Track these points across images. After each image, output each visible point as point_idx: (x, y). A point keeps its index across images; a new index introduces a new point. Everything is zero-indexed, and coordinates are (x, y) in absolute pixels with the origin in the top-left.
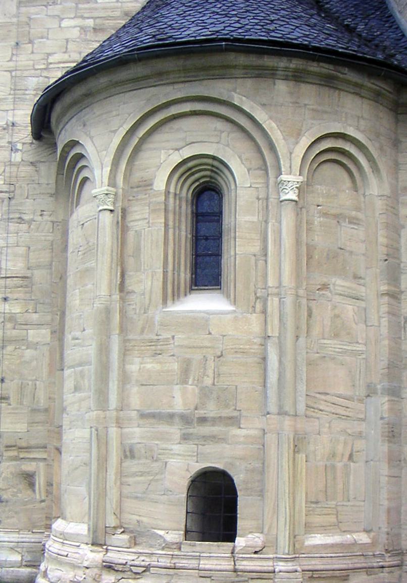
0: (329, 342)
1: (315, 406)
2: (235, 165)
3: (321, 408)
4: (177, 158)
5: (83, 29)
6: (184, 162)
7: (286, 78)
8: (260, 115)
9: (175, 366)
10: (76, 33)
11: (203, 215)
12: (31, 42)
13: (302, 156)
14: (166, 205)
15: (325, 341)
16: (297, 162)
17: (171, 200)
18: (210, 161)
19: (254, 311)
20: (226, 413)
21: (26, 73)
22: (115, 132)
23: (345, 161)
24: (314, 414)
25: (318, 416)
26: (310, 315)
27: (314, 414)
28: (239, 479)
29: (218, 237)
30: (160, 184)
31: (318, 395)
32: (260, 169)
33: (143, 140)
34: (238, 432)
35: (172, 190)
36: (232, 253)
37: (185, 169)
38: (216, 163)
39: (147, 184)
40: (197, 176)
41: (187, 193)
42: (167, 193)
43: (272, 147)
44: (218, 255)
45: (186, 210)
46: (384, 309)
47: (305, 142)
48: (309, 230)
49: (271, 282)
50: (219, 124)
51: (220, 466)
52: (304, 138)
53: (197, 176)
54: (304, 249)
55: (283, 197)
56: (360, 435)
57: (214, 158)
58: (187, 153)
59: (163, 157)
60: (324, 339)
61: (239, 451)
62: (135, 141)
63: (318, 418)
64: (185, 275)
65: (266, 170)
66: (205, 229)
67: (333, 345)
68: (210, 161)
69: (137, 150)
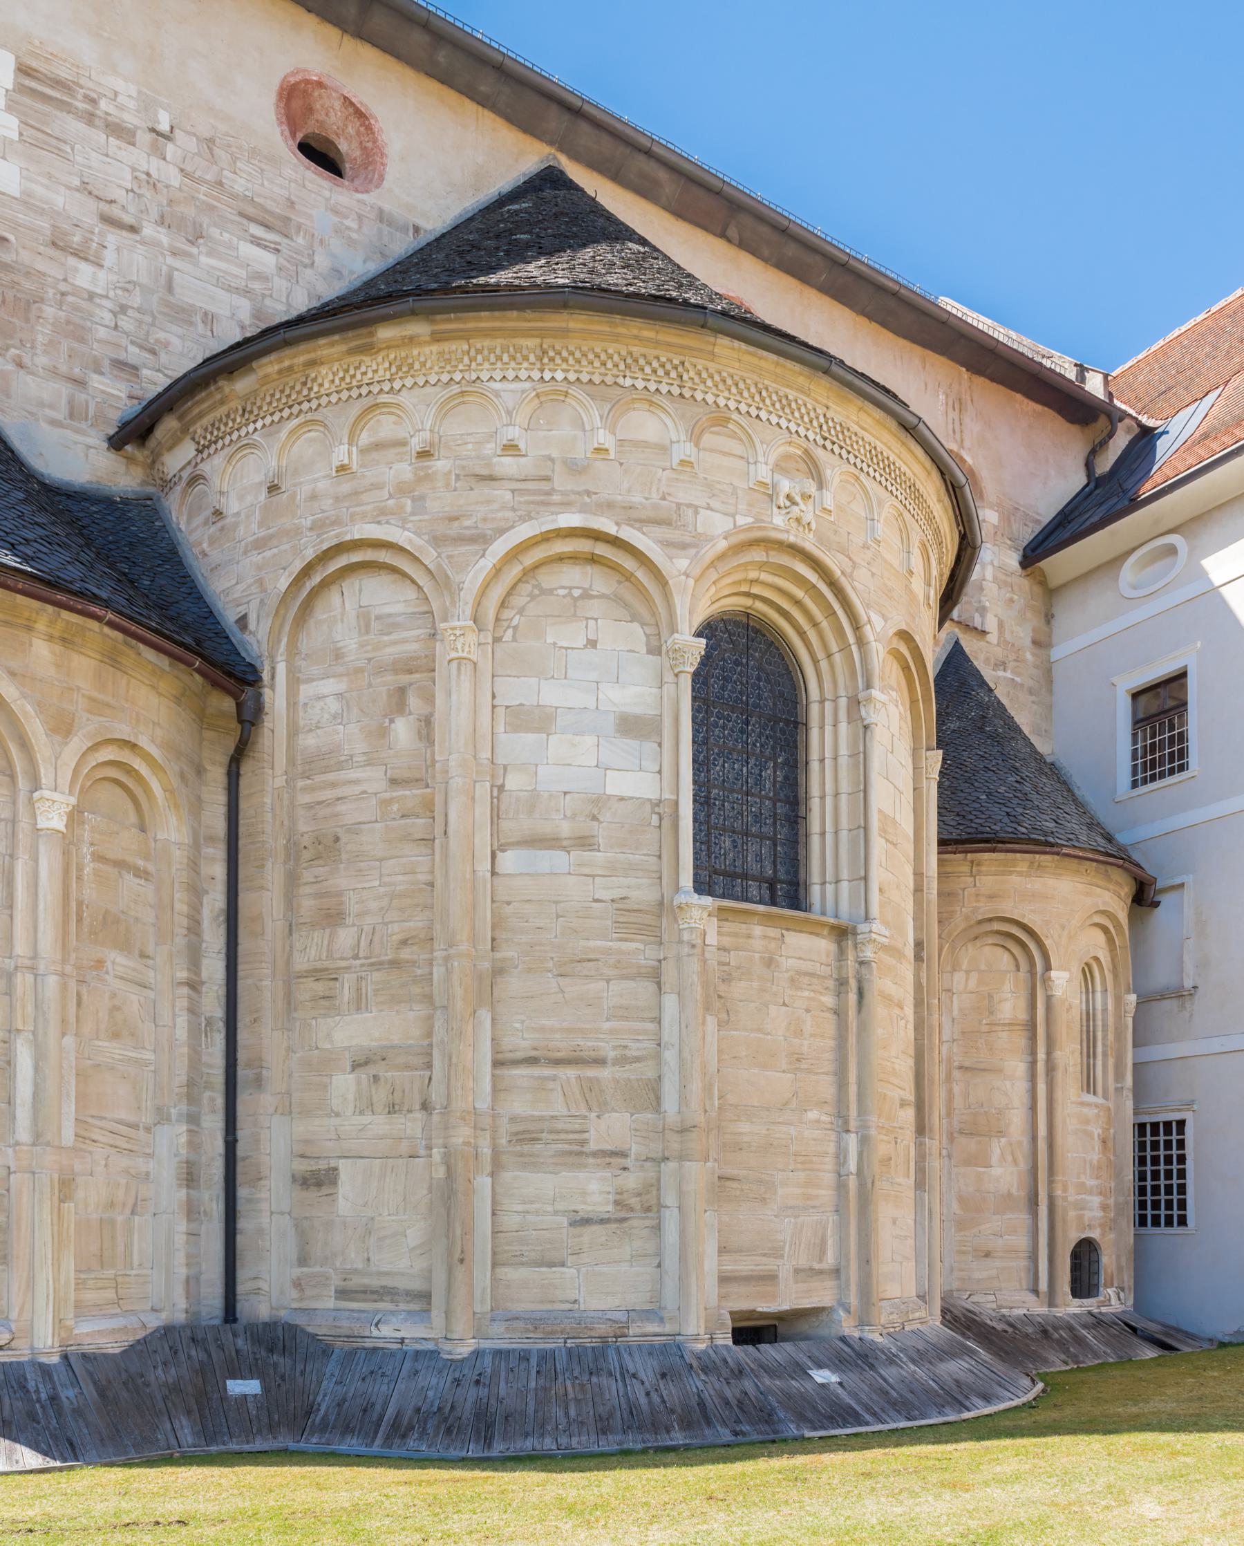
0: (106, 1044)
1: (86, 1134)
3: (95, 1138)
13: (73, 765)
15: (100, 1043)
24: (84, 1147)
25: (90, 1149)
26: (79, 1004)
27: (84, 1147)
31: (90, 1120)
48: (79, 878)
52: (76, 739)
54: (74, 905)
60: (97, 1039)
63: (91, 1153)
67: (112, 1050)
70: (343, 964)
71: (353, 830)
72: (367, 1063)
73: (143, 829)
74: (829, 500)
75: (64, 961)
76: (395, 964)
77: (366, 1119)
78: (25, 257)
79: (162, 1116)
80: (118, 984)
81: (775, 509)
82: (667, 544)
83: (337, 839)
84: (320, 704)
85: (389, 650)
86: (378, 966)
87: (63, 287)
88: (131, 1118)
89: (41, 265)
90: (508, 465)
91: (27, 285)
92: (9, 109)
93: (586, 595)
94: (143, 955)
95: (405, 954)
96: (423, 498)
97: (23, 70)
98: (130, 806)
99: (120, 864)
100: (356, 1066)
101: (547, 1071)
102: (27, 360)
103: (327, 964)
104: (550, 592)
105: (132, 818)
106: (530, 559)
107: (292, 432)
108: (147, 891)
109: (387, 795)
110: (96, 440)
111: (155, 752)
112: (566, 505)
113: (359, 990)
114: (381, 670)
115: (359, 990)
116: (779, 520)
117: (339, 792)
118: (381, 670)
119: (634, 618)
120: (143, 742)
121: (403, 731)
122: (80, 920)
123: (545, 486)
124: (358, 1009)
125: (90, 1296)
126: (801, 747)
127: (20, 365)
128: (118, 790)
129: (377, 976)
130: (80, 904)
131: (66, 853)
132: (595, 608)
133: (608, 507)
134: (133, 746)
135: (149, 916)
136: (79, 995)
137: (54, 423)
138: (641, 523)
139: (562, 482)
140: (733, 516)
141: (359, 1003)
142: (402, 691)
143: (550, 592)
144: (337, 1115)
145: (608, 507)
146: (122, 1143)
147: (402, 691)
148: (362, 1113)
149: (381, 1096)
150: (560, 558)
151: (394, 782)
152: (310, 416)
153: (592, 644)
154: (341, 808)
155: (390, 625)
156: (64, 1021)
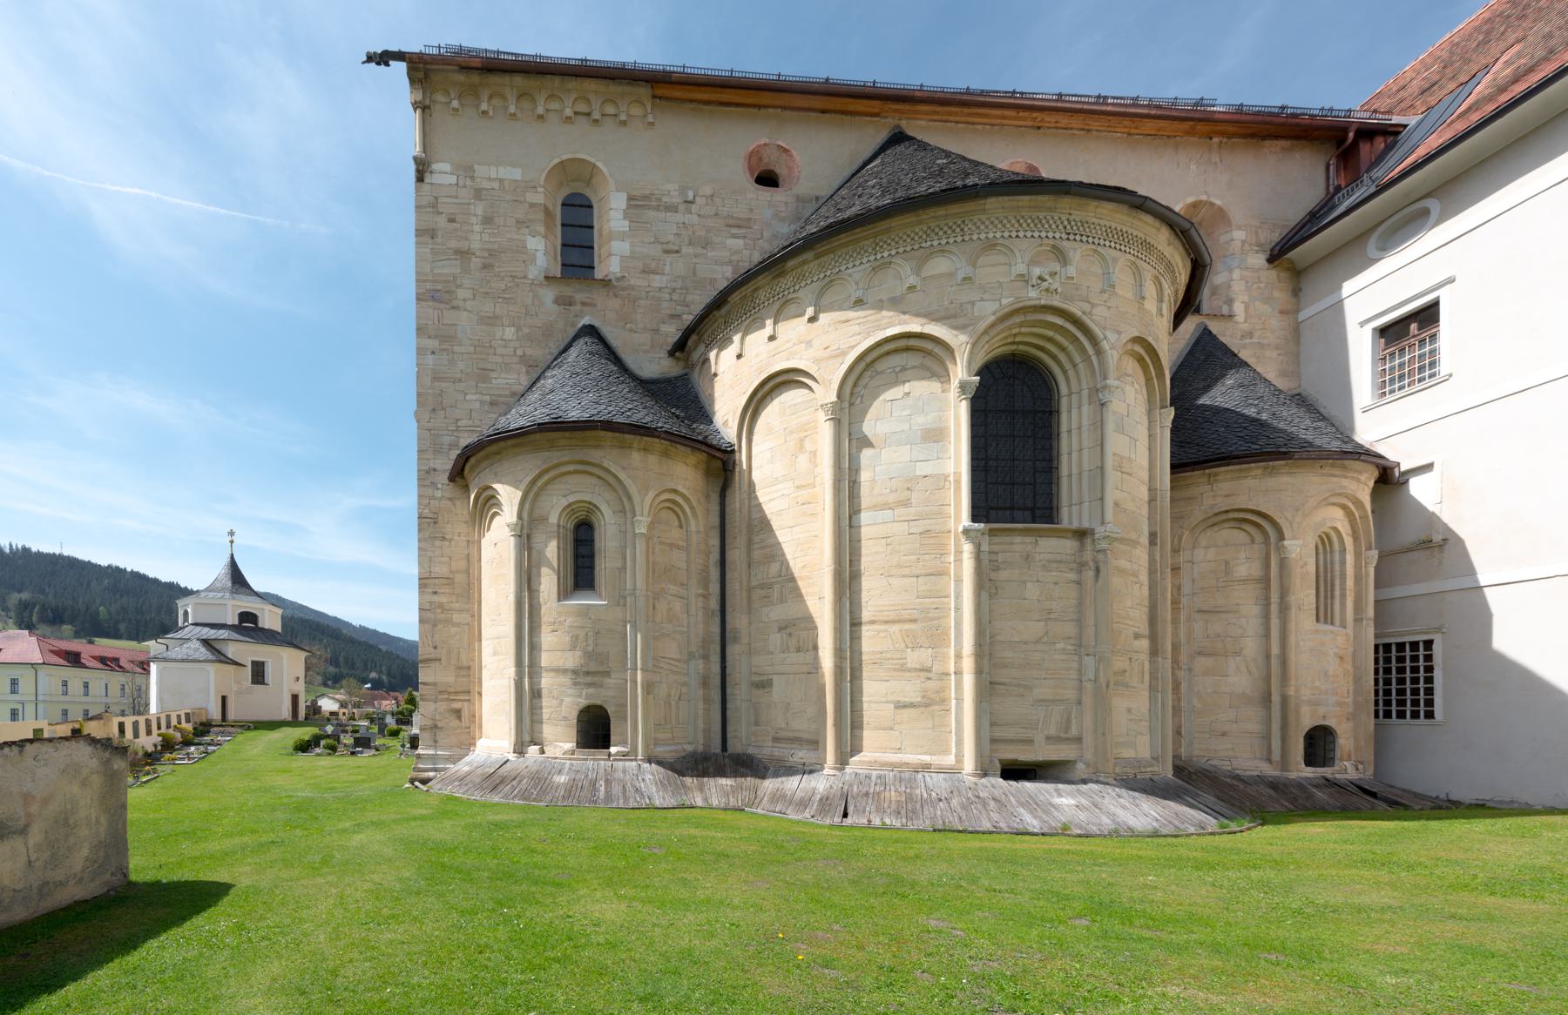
2: (604, 507)
4: (565, 502)
5: (482, 403)
6: (570, 505)
7: (639, 450)
8: (622, 476)
9: (568, 639)
10: (477, 405)
11: (581, 541)
12: (443, 409)
14: (559, 533)
16: (646, 511)
17: (561, 530)
18: (587, 505)
19: (619, 605)
20: (601, 669)
21: (440, 432)
22: (521, 481)
23: (676, 508)
26: (654, 608)
28: (611, 710)
29: (592, 556)
30: (553, 519)
32: (621, 512)
33: (541, 489)
34: (610, 681)
35: (561, 523)
36: (603, 566)
37: (570, 509)
38: (591, 507)
39: (544, 519)
40: (578, 514)
41: (570, 525)
42: (559, 526)
43: (630, 498)
44: (592, 567)
45: (570, 536)
46: (700, 604)
47: (651, 495)
48: (653, 553)
49: (629, 586)
50: (594, 480)
51: (598, 702)
53: (578, 514)
55: (637, 531)
56: (685, 684)
57: (590, 503)
58: (572, 499)
59: (555, 500)
61: (611, 693)
62: (535, 489)
64: (570, 581)
65: (625, 513)
66: (582, 550)
68: (587, 505)
69: (537, 495)
73: (681, 527)
74: (1071, 271)
75: (647, 590)
78: (632, 282)
79: (691, 656)
80: (670, 598)
81: (1030, 288)
87: (648, 289)
88: (679, 657)
89: (639, 282)
91: (633, 293)
92: (625, 218)
94: (682, 584)
98: (674, 517)
99: (672, 545)
102: (634, 327)
105: (677, 523)
106: (869, 359)
108: (683, 555)
110: (664, 354)
111: (685, 492)
116: (1033, 293)
120: (680, 488)
122: (654, 571)
125: (661, 736)
127: (631, 330)
128: (671, 513)
130: (654, 564)
131: (647, 543)
134: (675, 491)
135: (683, 565)
136: (654, 604)
137: (645, 352)
140: (1000, 300)
146: (673, 668)
150: (888, 353)
156: (647, 616)
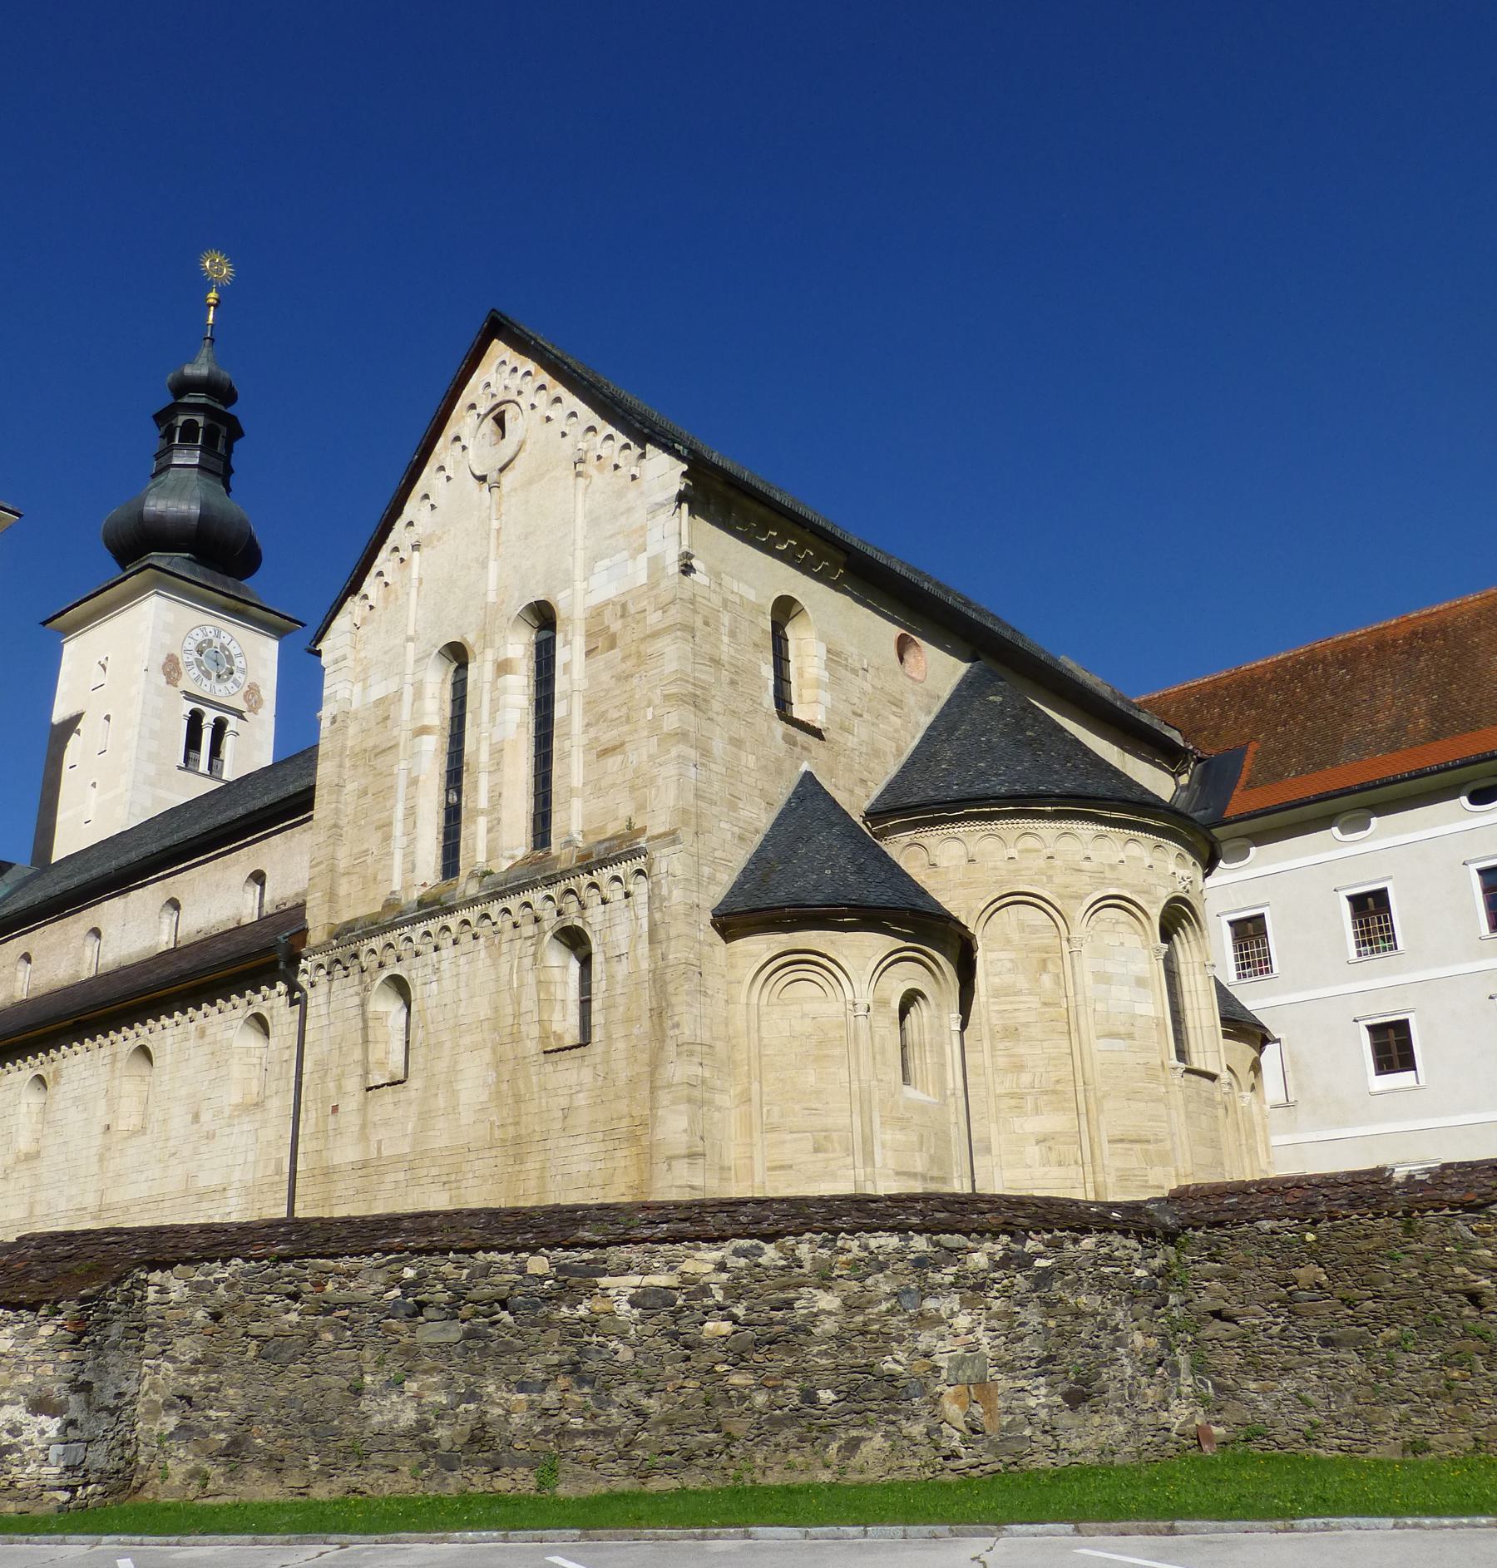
70: (1026, 1091)
71: (1027, 1025)
72: (1044, 1141)
76: (1054, 1092)
77: (1046, 1169)
82: (1149, 902)
83: (1017, 1030)
84: (1000, 963)
85: (1035, 941)
86: (1046, 1093)
90: (1086, 865)
93: (1117, 922)
95: (1059, 1087)
96: (1051, 876)
97: (829, 651)
100: (1038, 1142)
101: (1128, 1146)
103: (1018, 1091)
104: (1103, 920)
107: (982, 837)
109: (1042, 1010)
112: (1111, 885)
113: (1036, 1104)
114: (1034, 950)
115: (1036, 1104)
117: (1016, 1006)
118: (1034, 950)
119: (1136, 933)
121: (1047, 980)
123: (1102, 875)
124: (1037, 1114)
126: (1178, 984)
129: (1045, 1097)
132: (1120, 928)
133: (1126, 885)
138: (1139, 892)
139: (1108, 874)
141: (1037, 1111)
142: (1044, 961)
143: (1103, 920)
144: (1030, 1167)
145: (1126, 885)
147: (1044, 961)
148: (1044, 1166)
149: (1053, 1157)
151: (1045, 1004)
152: (992, 832)
153: (1122, 944)
154: (1017, 1014)
155: (1035, 930)
